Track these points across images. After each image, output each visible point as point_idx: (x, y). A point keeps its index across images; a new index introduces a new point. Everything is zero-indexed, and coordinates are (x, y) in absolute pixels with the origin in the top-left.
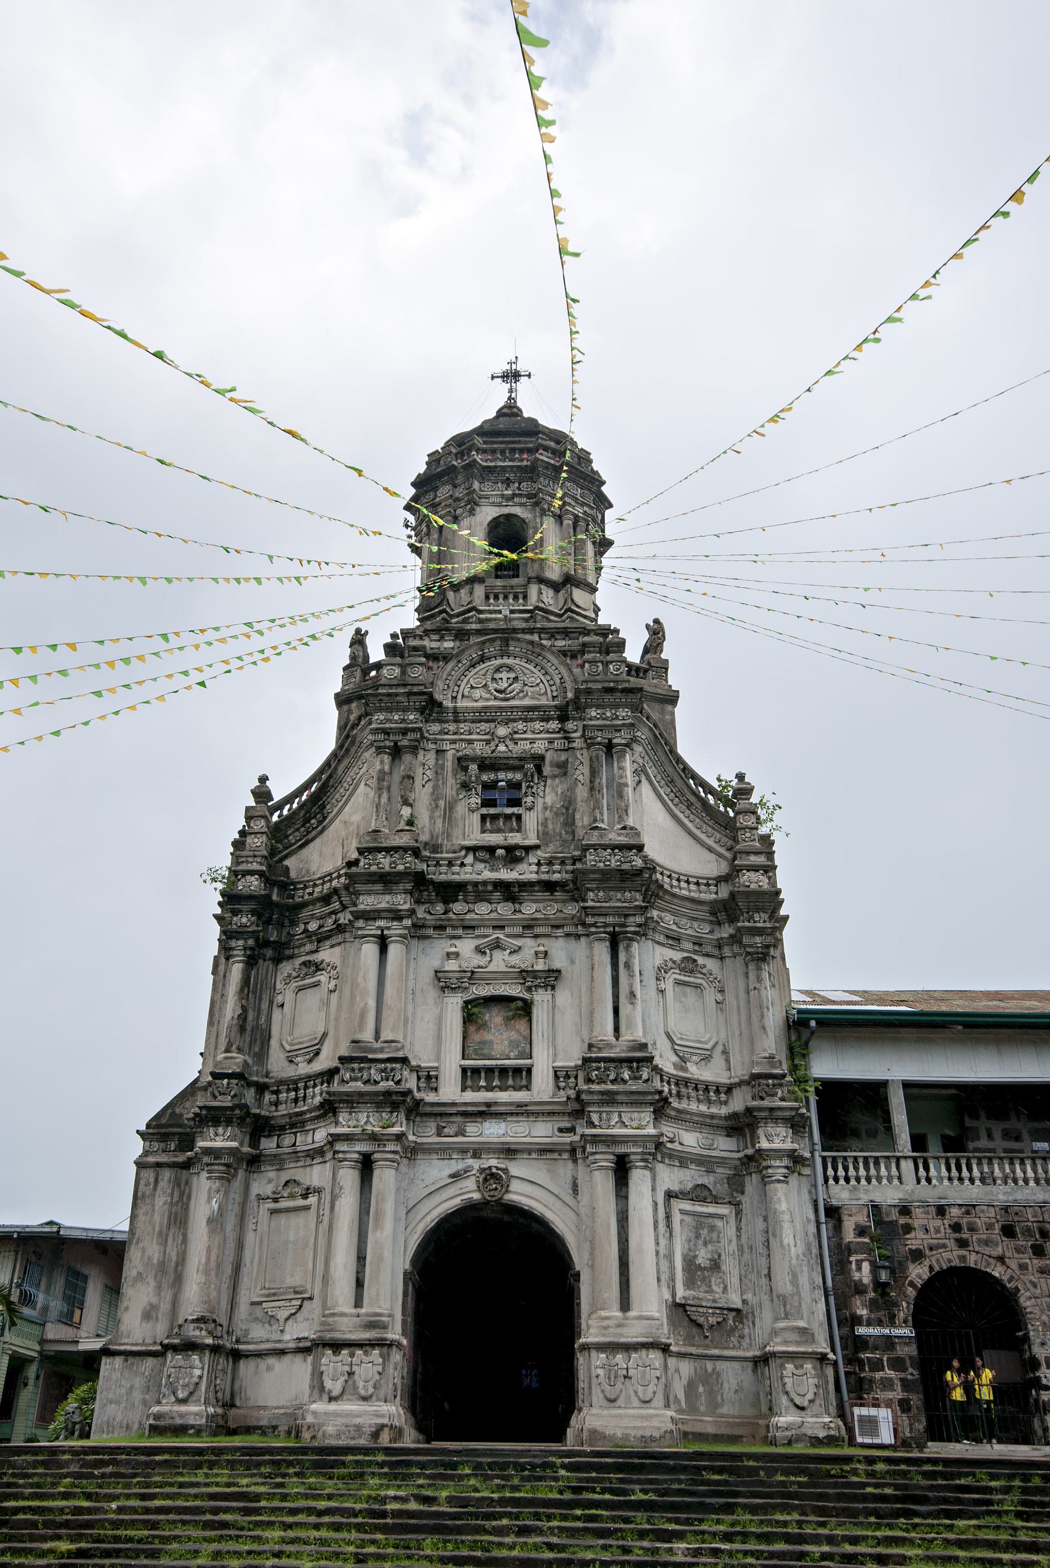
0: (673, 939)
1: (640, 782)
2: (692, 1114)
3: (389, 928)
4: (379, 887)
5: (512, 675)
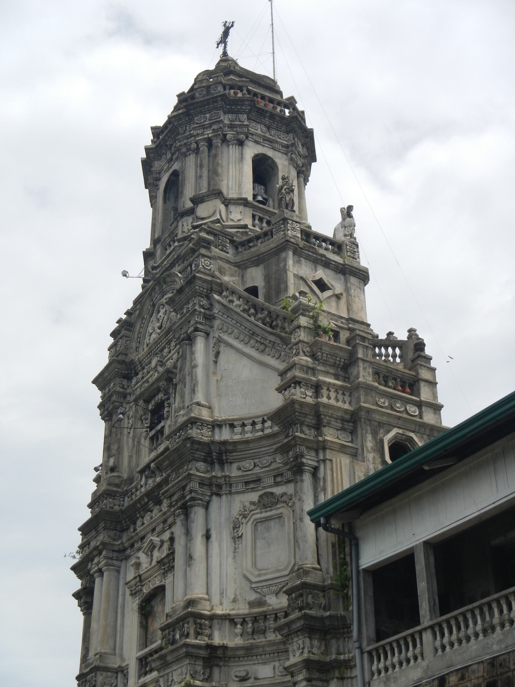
0: (254, 481)
1: (217, 354)
2: (263, 646)
3: (99, 562)
4: (93, 533)
5: (164, 310)
